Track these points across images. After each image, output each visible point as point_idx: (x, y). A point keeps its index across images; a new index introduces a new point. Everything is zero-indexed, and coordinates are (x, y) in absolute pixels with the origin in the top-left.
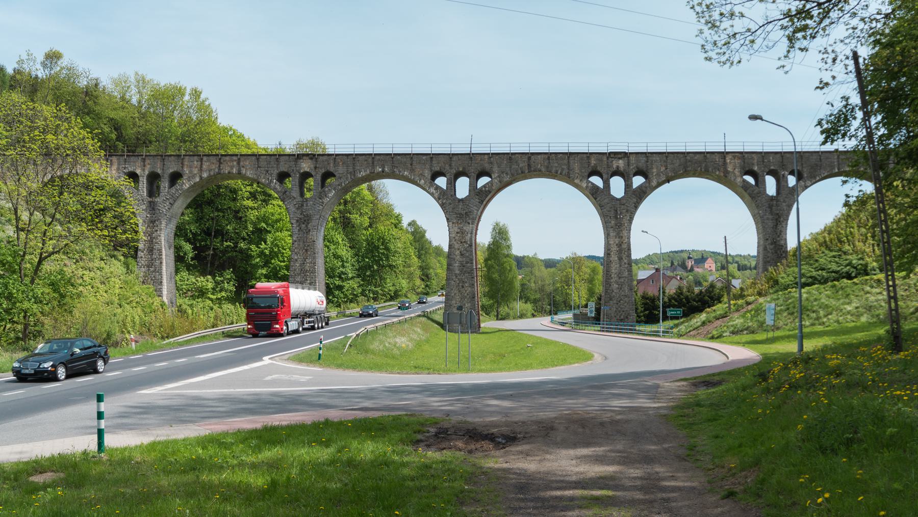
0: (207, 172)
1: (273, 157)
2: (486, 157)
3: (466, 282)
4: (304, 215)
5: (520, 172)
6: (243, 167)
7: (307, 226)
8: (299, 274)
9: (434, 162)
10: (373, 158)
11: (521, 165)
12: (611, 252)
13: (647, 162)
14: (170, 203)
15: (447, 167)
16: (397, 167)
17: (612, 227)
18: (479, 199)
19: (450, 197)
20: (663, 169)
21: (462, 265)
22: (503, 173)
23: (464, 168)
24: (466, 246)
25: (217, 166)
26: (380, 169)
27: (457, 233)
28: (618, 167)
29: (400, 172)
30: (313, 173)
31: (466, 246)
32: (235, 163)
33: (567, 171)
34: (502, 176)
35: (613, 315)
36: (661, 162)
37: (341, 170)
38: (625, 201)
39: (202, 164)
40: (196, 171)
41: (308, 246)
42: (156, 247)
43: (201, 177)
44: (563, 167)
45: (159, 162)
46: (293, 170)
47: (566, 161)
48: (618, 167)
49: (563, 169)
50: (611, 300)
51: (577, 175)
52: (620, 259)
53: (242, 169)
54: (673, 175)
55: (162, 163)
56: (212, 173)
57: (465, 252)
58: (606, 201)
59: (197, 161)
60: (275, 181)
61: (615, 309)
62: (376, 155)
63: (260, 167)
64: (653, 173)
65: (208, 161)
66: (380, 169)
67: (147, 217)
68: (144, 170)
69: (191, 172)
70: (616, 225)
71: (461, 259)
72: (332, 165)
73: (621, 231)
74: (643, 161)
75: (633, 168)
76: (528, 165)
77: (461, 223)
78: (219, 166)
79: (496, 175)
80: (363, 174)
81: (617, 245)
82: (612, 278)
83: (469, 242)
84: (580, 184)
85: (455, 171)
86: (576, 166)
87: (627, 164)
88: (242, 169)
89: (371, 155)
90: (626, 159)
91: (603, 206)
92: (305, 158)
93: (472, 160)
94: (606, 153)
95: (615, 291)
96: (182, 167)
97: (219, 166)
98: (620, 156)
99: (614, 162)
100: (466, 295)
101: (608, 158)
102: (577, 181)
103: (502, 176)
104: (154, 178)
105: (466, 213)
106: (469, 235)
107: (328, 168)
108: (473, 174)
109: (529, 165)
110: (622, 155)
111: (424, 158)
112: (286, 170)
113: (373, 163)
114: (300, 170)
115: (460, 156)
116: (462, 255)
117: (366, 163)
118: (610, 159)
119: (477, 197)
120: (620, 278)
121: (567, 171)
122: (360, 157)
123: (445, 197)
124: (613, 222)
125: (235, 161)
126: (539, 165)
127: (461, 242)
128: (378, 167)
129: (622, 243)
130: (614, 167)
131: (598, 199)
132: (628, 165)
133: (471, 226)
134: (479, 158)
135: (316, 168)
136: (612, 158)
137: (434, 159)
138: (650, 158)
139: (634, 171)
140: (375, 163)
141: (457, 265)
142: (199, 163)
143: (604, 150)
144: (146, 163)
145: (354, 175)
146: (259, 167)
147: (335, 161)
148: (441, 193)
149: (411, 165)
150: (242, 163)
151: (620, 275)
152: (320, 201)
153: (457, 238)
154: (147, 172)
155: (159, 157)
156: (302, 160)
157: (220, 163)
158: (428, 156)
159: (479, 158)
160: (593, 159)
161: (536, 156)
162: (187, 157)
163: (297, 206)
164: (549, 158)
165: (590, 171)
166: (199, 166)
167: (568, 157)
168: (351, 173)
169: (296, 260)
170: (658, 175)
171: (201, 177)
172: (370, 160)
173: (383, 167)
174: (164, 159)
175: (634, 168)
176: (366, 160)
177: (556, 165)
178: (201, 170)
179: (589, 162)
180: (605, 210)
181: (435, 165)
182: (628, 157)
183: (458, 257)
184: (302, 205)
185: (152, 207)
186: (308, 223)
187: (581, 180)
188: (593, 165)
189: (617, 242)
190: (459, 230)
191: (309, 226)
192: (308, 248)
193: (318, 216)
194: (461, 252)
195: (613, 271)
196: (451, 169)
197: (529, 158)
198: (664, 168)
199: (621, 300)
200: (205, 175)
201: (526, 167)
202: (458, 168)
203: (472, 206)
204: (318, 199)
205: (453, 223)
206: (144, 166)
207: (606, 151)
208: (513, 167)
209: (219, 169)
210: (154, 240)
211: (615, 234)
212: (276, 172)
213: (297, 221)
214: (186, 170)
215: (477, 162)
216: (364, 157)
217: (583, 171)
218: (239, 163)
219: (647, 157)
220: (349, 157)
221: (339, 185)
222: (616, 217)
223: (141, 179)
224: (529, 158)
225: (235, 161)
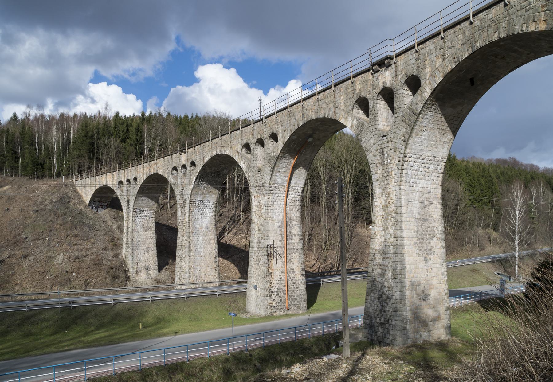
17: (378, 180)
52: (386, 228)
54: (454, 66)
58: (372, 141)
64: (425, 75)
73: (388, 184)
83: (264, 217)
130: (381, 84)
149: (231, 142)
151: (384, 255)
170: (433, 76)
183: (257, 232)
209: (150, 172)
218: (157, 166)
222: (382, 164)
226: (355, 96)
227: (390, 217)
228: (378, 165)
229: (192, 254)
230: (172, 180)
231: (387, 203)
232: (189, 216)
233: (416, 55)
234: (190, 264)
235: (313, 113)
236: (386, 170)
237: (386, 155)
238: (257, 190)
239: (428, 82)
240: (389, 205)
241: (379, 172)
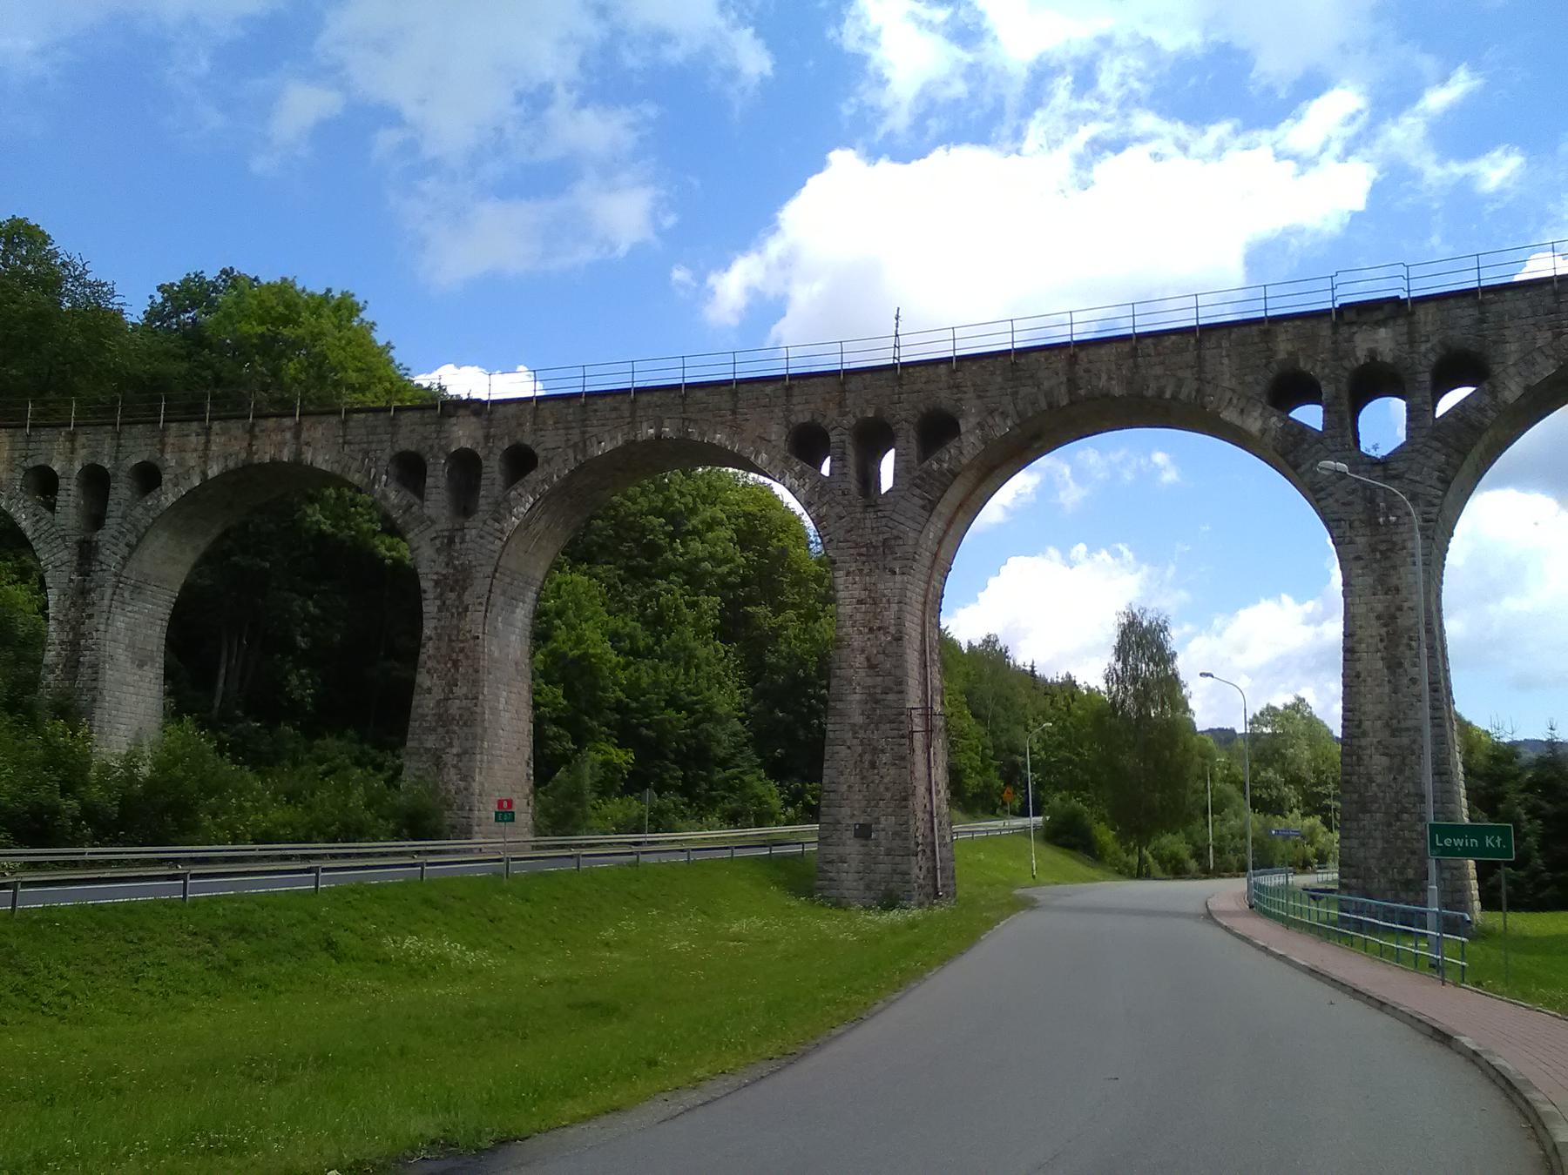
0: (221, 460)
1: (382, 415)
2: (943, 368)
3: (883, 751)
4: (455, 567)
5: (1044, 405)
6: (308, 444)
7: (460, 597)
8: (433, 730)
9: (794, 400)
10: (634, 402)
11: (1046, 385)
12: (1360, 642)
13: (1483, 321)
14: (127, 545)
15: (833, 413)
16: (695, 421)
17: (1358, 558)
18: (923, 498)
19: (839, 499)
20: (1543, 338)
21: (873, 699)
22: (991, 413)
23: (879, 410)
24: (885, 639)
25: (245, 444)
26: (651, 431)
27: (860, 602)
28: (1372, 354)
29: (703, 434)
30: (481, 453)
31: (885, 639)
32: (288, 435)
33: (1195, 385)
34: (991, 422)
35: (1372, 862)
36: (1534, 314)
37: (547, 442)
38: (1402, 466)
39: (208, 442)
40: (192, 459)
41: (462, 650)
42: (87, 658)
43: (204, 474)
44: (1180, 374)
45: (108, 440)
46: (431, 447)
47: (1189, 356)
48: (1372, 354)
49: (1180, 383)
50: (1364, 810)
51: (1228, 395)
52: (1394, 665)
53: (305, 448)
55: (115, 442)
56: (231, 464)
57: (881, 657)
59: (198, 435)
60: (384, 477)
61: (1380, 844)
62: (639, 391)
63: (350, 443)
65: (224, 432)
66: (651, 431)
67: (71, 581)
68: (71, 461)
69: (181, 463)
70: (1374, 550)
71: (869, 681)
72: (528, 427)
73: (1394, 567)
74: (1467, 321)
75: (1427, 355)
76: (1069, 380)
77: (870, 574)
78: (250, 445)
79: (973, 421)
80: (606, 446)
81: (1378, 618)
82: (1364, 734)
83: (892, 630)
84: (1238, 422)
85: (853, 422)
86: (1223, 365)
87: (1404, 339)
88: (305, 448)
89: (626, 391)
90: (1400, 321)
91: (1322, 489)
92: (461, 412)
93: (901, 385)
94: (1327, 312)
95: (1379, 779)
96: (162, 451)
97: (250, 445)
98: (1380, 315)
99: (1358, 338)
100: (882, 789)
101: (1335, 326)
102: (1229, 415)
103: (991, 422)
104: (96, 481)
105: (885, 540)
106: (895, 607)
107: (519, 437)
108: (905, 425)
109: (1072, 383)
110: (1387, 308)
111: (769, 389)
112: (413, 449)
113: (633, 414)
114: (448, 446)
115: (868, 376)
116: (872, 666)
117: (614, 415)
118: (1344, 331)
119: (917, 492)
120: (1395, 732)
121: (1195, 385)
122: (600, 402)
123: (827, 498)
124: (1361, 541)
125: (290, 428)
126: (1104, 377)
127: (871, 630)
128: (645, 425)
129: (1400, 609)
131: (1303, 468)
132: (1412, 342)
133: (898, 578)
134: (923, 373)
135: (487, 437)
136: (1351, 324)
137: (796, 391)
138: (1494, 308)
139: (1433, 358)
140: (640, 413)
141: (857, 697)
142: (202, 439)
143: (1322, 302)
144: (77, 445)
145: (584, 451)
146: (345, 443)
147: (535, 417)
148: (813, 488)
149: (734, 412)
150: (304, 436)
152: (497, 525)
153: (858, 616)
154: (78, 467)
155: (110, 428)
156: (453, 420)
157: (253, 437)
158: (779, 385)
159: (923, 373)
160: (1282, 337)
161: (1092, 351)
162: (173, 425)
163: (438, 542)
164: (1134, 353)
165: (1271, 376)
166: (201, 448)
167: (1199, 341)
168: (575, 445)
169: (429, 691)
171: (204, 474)
172: (625, 407)
173: (659, 425)
174: (119, 434)
175: (1433, 349)
176: (615, 409)
177: (1158, 370)
178: (205, 458)
179: (1269, 349)
180: (1331, 500)
181: (799, 408)
182: (1412, 314)
183: (862, 673)
184: (451, 541)
185: (87, 553)
186: (464, 589)
187: (1242, 411)
188: (1282, 356)
189: (1380, 608)
190: (864, 595)
191: (467, 598)
192: (461, 656)
193: (490, 570)
194: (868, 659)
195: (1368, 708)
196: (845, 414)
197: (1073, 360)
198: (1549, 334)
199: (1404, 810)
200: (214, 470)
201: (1063, 389)
202: (863, 412)
203: (902, 519)
204: (490, 522)
205: (848, 574)
206: (73, 451)
207: (1329, 306)
208: (1023, 391)
209: (250, 453)
210: (83, 642)
211: (1370, 580)
212: (386, 457)
213: (437, 583)
214: (171, 459)
215: (916, 387)
216: (609, 399)
217: (1249, 379)
218: (297, 436)
219: (1482, 303)
220: (573, 402)
221: (543, 481)
222: (1371, 523)
223: (62, 482)
224: (1073, 360)
225: (290, 428)
226: (1274, 365)
227: (1405, 641)
228: (1357, 524)
230: (392, 495)
231: (1393, 609)
232: (485, 617)
233: (1475, 312)
235: (1114, 382)
236: (1383, 537)
237: (1382, 504)
238: (860, 555)
239: (1512, 370)
240: (1398, 613)
241: (1361, 541)
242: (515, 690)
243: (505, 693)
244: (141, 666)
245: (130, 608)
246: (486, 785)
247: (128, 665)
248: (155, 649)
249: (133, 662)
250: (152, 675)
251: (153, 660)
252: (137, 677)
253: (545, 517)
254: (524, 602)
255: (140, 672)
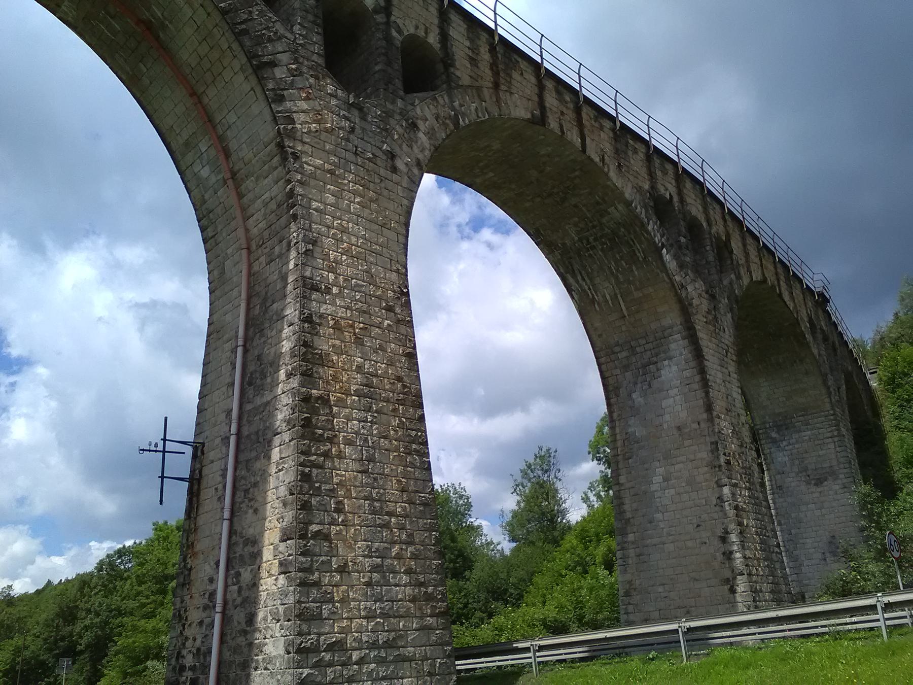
229: (631, 537)
234: (628, 577)
242: (683, 458)
243: (661, 470)
244: (819, 482)
245: (785, 443)
246: (638, 582)
247: (803, 487)
248: (834, 463)
249: (808, 483)
250: (837, 487)
251: (833, 474)
252: (817, 495)
253: (597, 280)
254: (670, 358)
255: (819, 490)
